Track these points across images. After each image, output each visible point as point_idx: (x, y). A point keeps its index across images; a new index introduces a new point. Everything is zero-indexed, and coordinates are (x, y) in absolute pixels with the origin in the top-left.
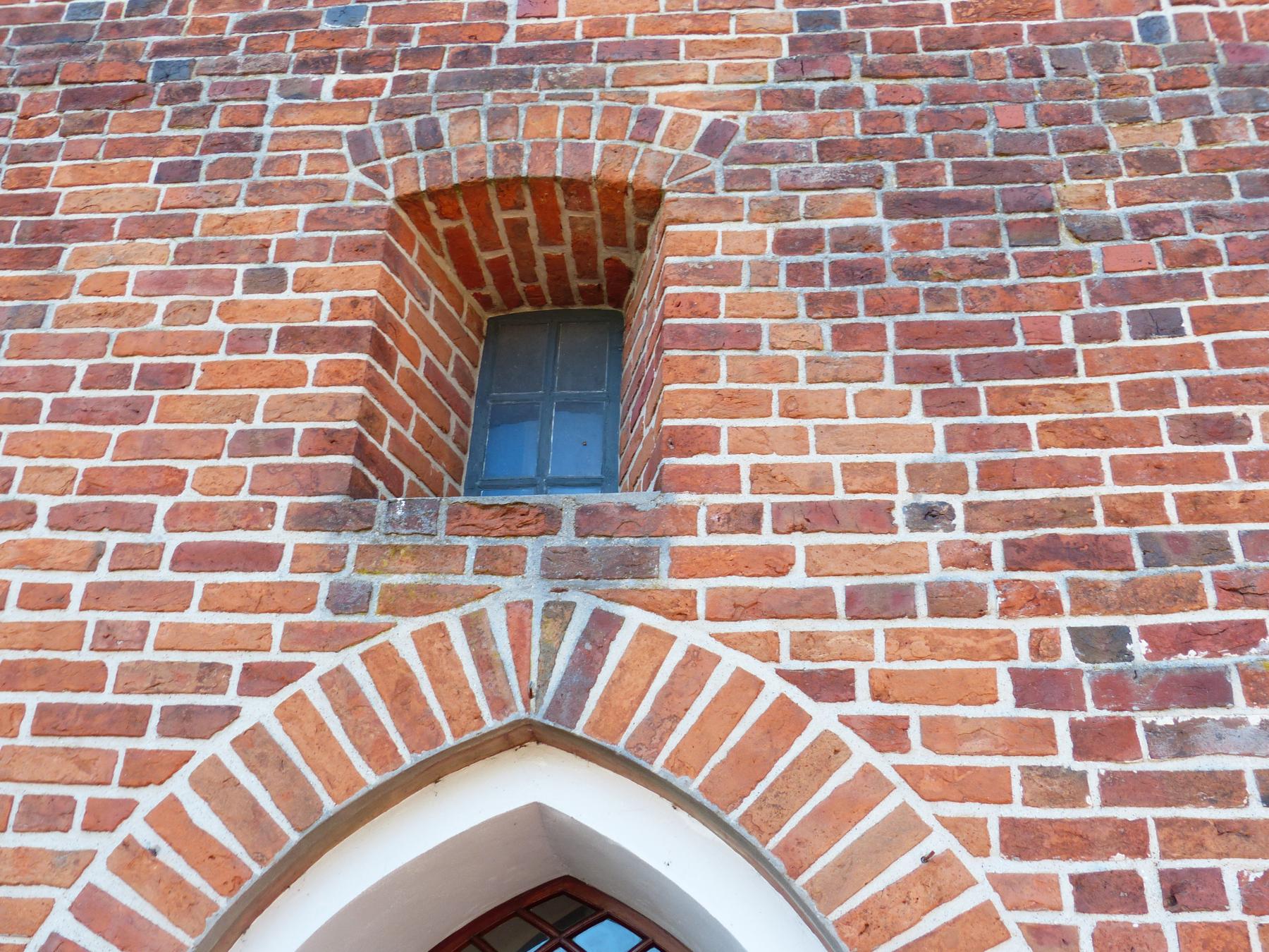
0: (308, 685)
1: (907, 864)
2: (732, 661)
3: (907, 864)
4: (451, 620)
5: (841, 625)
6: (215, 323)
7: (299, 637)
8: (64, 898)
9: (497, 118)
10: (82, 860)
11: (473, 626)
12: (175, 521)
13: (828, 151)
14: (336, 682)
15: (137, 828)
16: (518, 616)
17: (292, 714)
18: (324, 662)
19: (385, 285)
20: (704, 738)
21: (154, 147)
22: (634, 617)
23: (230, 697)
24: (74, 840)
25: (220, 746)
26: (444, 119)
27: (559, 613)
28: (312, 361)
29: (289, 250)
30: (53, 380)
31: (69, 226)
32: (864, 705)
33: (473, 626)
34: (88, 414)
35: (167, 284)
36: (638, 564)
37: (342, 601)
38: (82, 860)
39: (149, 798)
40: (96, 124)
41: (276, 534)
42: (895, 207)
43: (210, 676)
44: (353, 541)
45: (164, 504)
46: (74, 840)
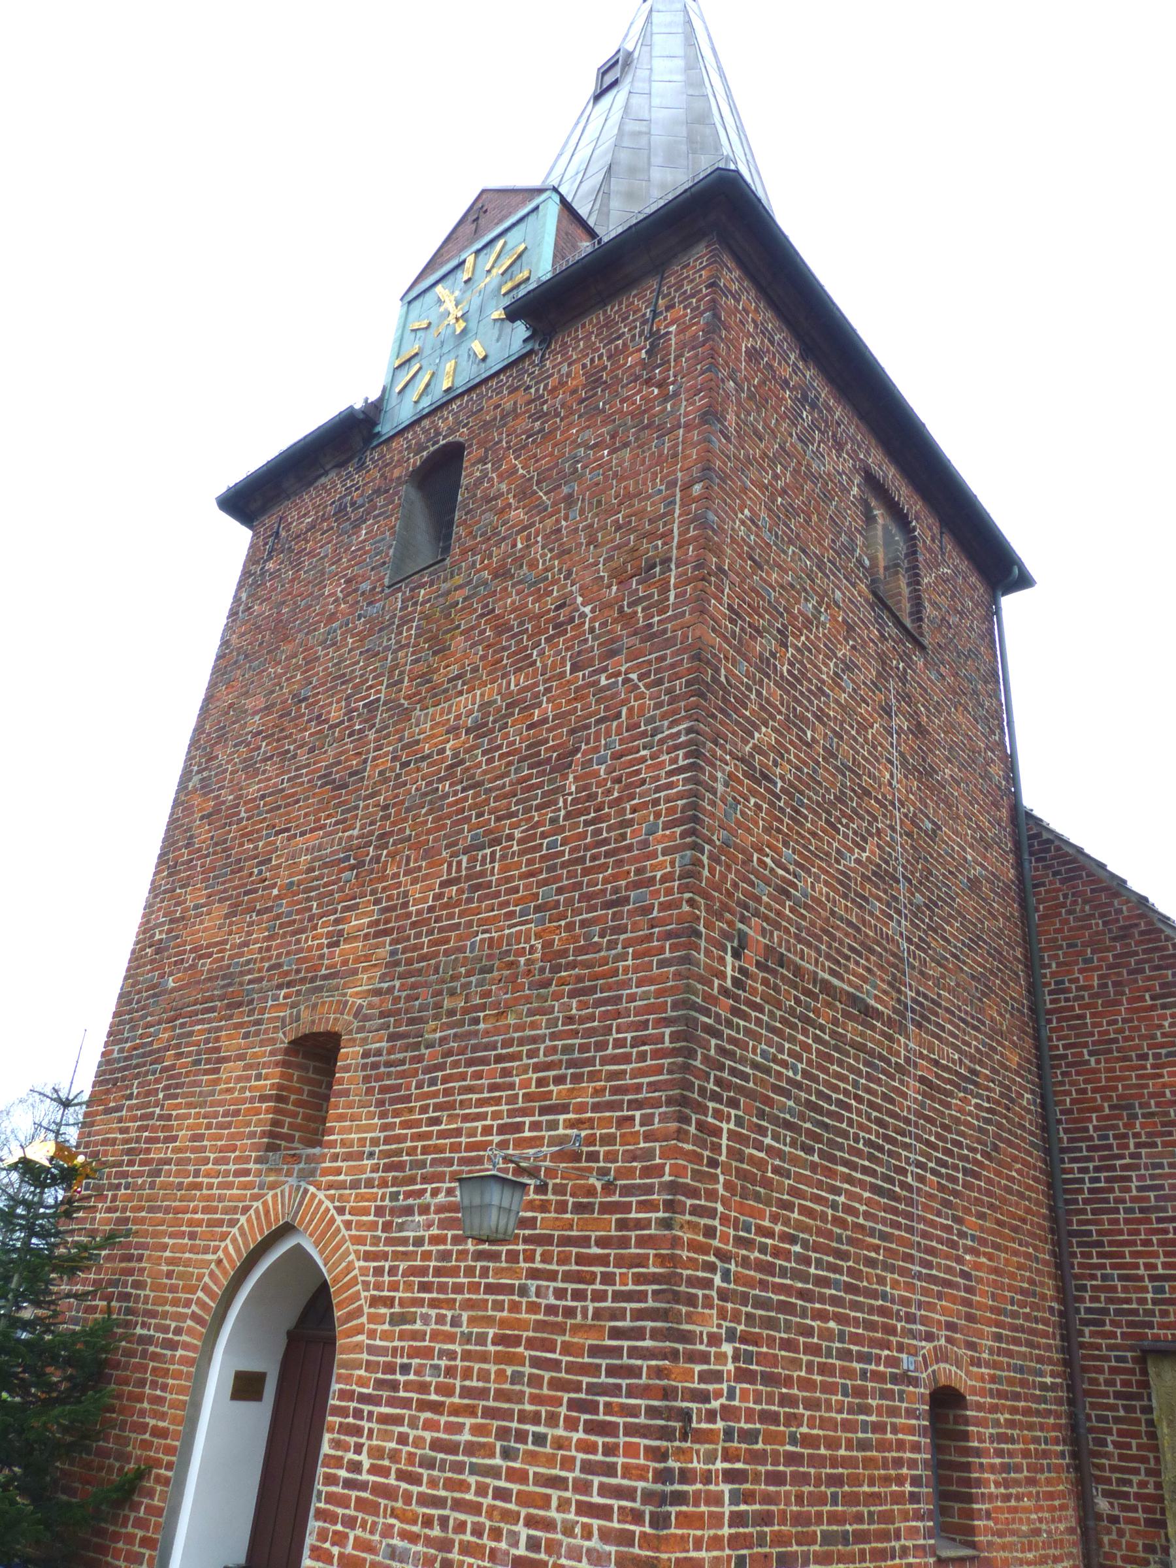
0: (252, 1212)
2: (327, 1203)
14: (257, 1211)
15: (220, 1253)
17: (249, 1220)
19: (282, 1076)
20: (316, 1228)
22: (312, 1189)
25: (235, 1230)
27: (299, 1187)
36: (312, 1173)
40: (231, 1017)
41: (252, 1166)
44: (264, 1167)
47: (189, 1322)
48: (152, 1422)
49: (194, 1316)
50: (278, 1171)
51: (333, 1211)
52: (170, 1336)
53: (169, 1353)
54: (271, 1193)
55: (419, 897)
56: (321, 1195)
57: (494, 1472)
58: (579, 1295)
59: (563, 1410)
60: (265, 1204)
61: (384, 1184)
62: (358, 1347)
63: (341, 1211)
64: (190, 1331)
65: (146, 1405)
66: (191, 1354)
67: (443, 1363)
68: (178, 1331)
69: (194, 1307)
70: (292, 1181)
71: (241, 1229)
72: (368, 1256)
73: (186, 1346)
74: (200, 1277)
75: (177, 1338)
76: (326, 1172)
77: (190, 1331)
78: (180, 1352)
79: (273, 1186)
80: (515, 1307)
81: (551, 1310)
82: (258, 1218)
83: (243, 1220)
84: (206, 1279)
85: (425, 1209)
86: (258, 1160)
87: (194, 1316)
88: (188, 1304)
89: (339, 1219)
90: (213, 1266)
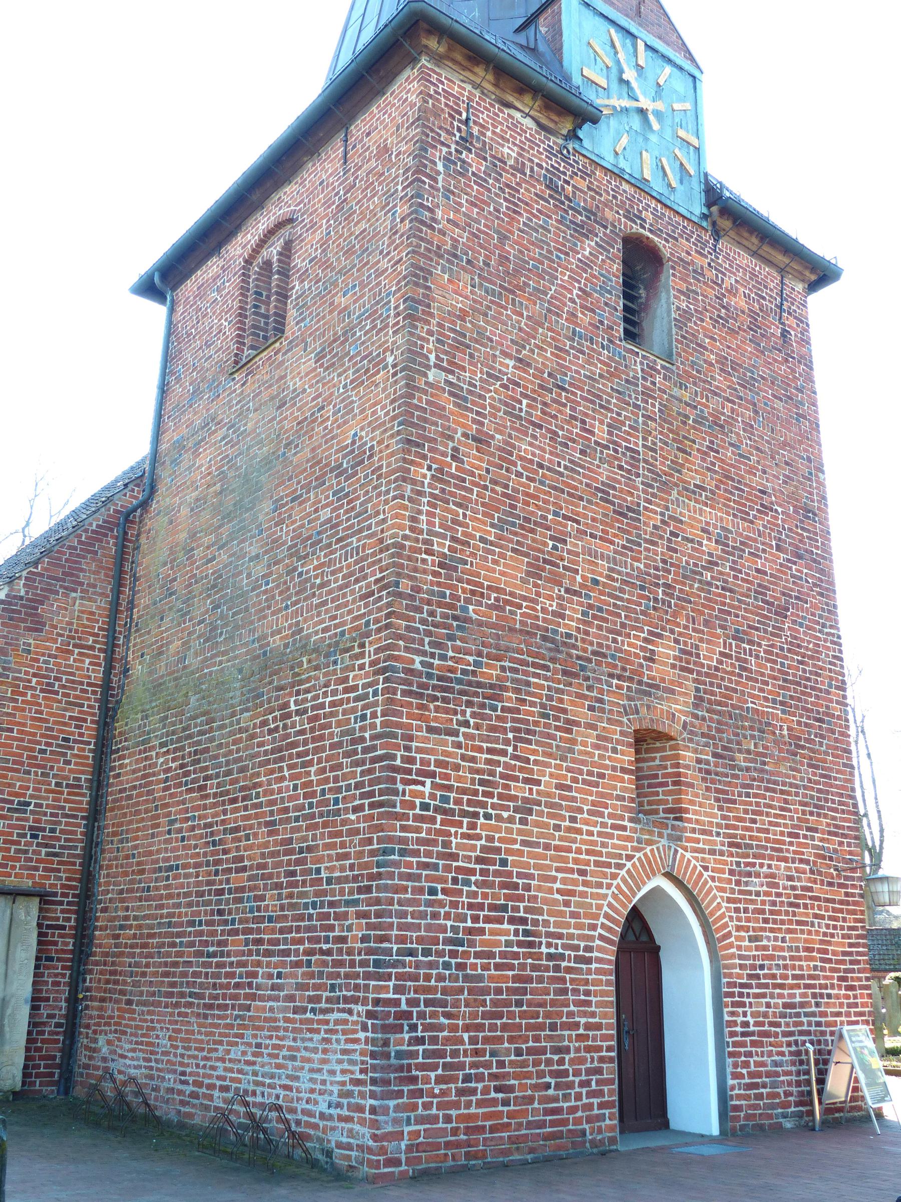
0: (635, 860)
1: (715, 904)
2: (694, 862)
3: (715, 904)
4: (654, 847)
5: (707, 856)
6: (607, 762)
7: (634, 849)
8: (606, 903)
9: (649, 707)
10: (607, 895)
11: (658, 849)
12: (610, 816)
13: (703, 735)
14: (639, 859)
15: (613, 889)
16: (664, 846)
17: (634, 865)
18: (638, 855)
21: (585, 697)
22: (680, 851)
23: (624, 862)
24: (604, 891)
25: (623, 872)
26: (638, 703)
27: (670, 847)
28: (626, 777)
29: (618, 742)
30: (581, 772)
31: (574, 721)
32: (710, 873)
33: (658, 849)
34: (590, 783)
35: (596, 747)
37: (639, 841)
38: (607, 895)
39: (615, 883)
40: (570, 685)
41: (626, 823)
42: (715, 755)
43: (620, 856)
45: (606, 812)
46: (604, 891)
47: (598, 942)
48: (583, 1020)
49: (601, 938)
50: (651, 833)
51: (699, 868)
52: (581, 953)
53: (584, 966)
54: (649, 848)
55: (709, 656)
56: (688, 855)
57: (813, 1014)
58: (835, 927)
59: (835, 981)
60: (645, 855)
61: (731, 855)
62: (733, 956)
63: (706, 868)
64: (600, 949)
65: (572, 1008)
66: (606, 966)
67: (781, 962)
68: (588, 949)
69: (599, 930)
70: (664, 842)
71: (628, 871)
72: (729, 900)
73: (599, 960)
74: (599, 907)
75: (587, 955)
76: (689, 840)
77: (600, 949)
78: (594, 966)
79: (649, 843)
80: (810, 932)
81: (825, 934)
82: (643, 866)
83: (629, 865)
84: (606, 908)
85: (758, 875)
86: (631, 820)
87: (601, 938)
88: (593, 927)
89: (706, 874)
90: (610, 899)
